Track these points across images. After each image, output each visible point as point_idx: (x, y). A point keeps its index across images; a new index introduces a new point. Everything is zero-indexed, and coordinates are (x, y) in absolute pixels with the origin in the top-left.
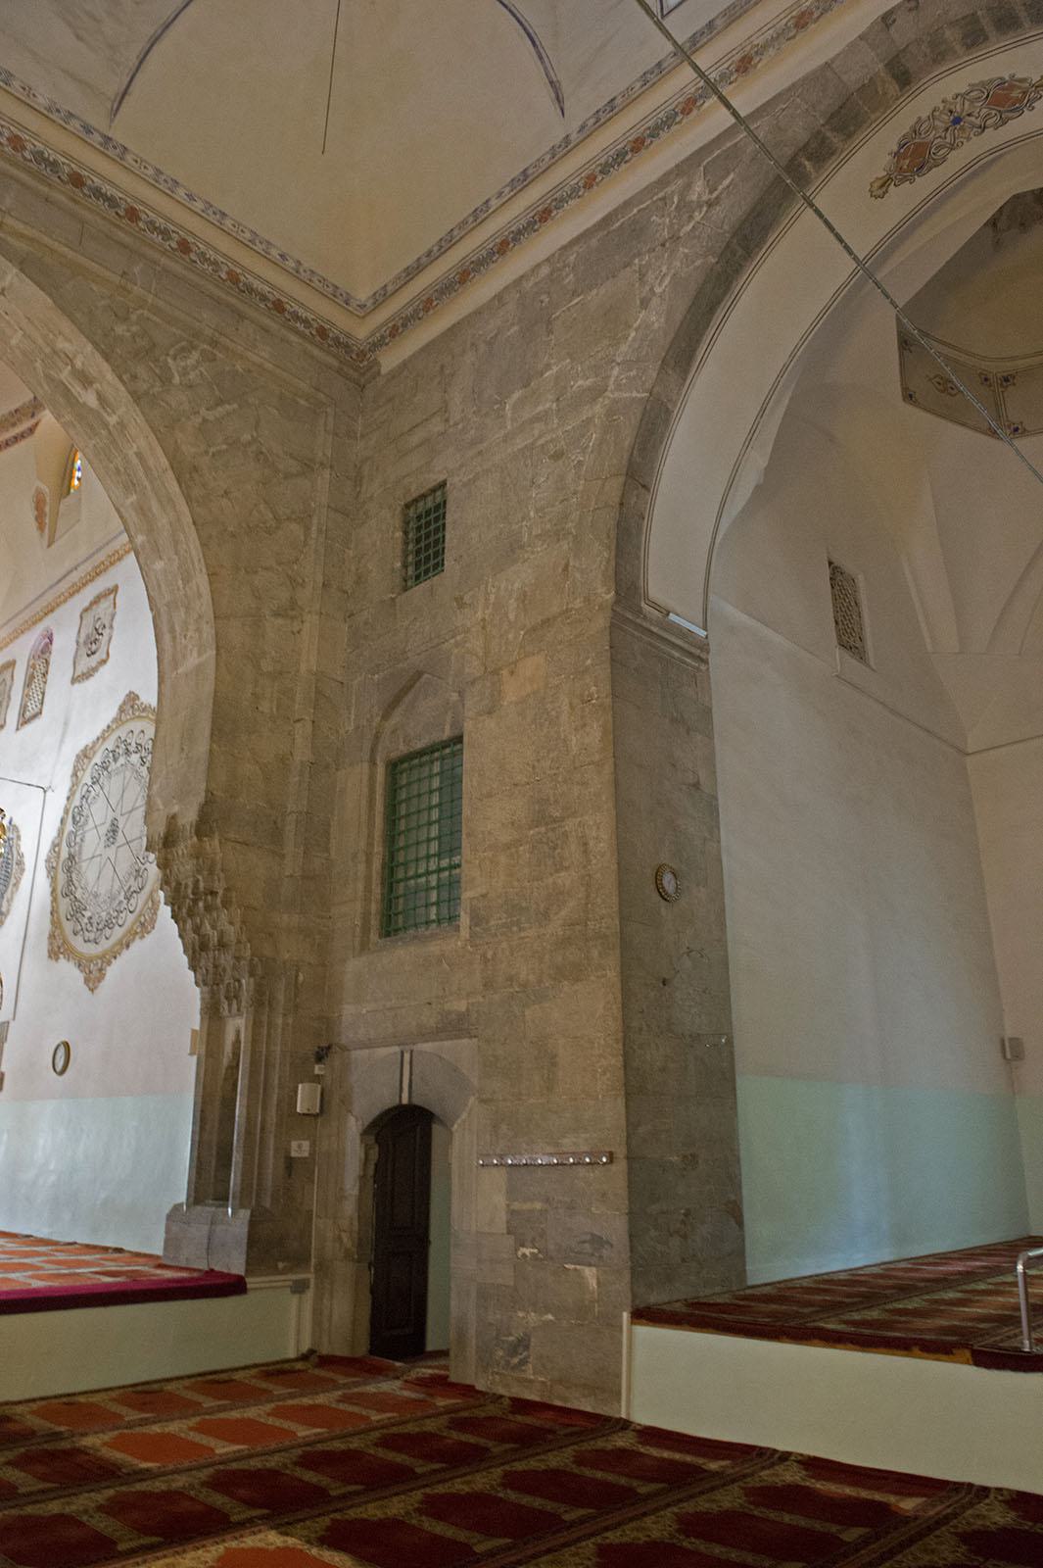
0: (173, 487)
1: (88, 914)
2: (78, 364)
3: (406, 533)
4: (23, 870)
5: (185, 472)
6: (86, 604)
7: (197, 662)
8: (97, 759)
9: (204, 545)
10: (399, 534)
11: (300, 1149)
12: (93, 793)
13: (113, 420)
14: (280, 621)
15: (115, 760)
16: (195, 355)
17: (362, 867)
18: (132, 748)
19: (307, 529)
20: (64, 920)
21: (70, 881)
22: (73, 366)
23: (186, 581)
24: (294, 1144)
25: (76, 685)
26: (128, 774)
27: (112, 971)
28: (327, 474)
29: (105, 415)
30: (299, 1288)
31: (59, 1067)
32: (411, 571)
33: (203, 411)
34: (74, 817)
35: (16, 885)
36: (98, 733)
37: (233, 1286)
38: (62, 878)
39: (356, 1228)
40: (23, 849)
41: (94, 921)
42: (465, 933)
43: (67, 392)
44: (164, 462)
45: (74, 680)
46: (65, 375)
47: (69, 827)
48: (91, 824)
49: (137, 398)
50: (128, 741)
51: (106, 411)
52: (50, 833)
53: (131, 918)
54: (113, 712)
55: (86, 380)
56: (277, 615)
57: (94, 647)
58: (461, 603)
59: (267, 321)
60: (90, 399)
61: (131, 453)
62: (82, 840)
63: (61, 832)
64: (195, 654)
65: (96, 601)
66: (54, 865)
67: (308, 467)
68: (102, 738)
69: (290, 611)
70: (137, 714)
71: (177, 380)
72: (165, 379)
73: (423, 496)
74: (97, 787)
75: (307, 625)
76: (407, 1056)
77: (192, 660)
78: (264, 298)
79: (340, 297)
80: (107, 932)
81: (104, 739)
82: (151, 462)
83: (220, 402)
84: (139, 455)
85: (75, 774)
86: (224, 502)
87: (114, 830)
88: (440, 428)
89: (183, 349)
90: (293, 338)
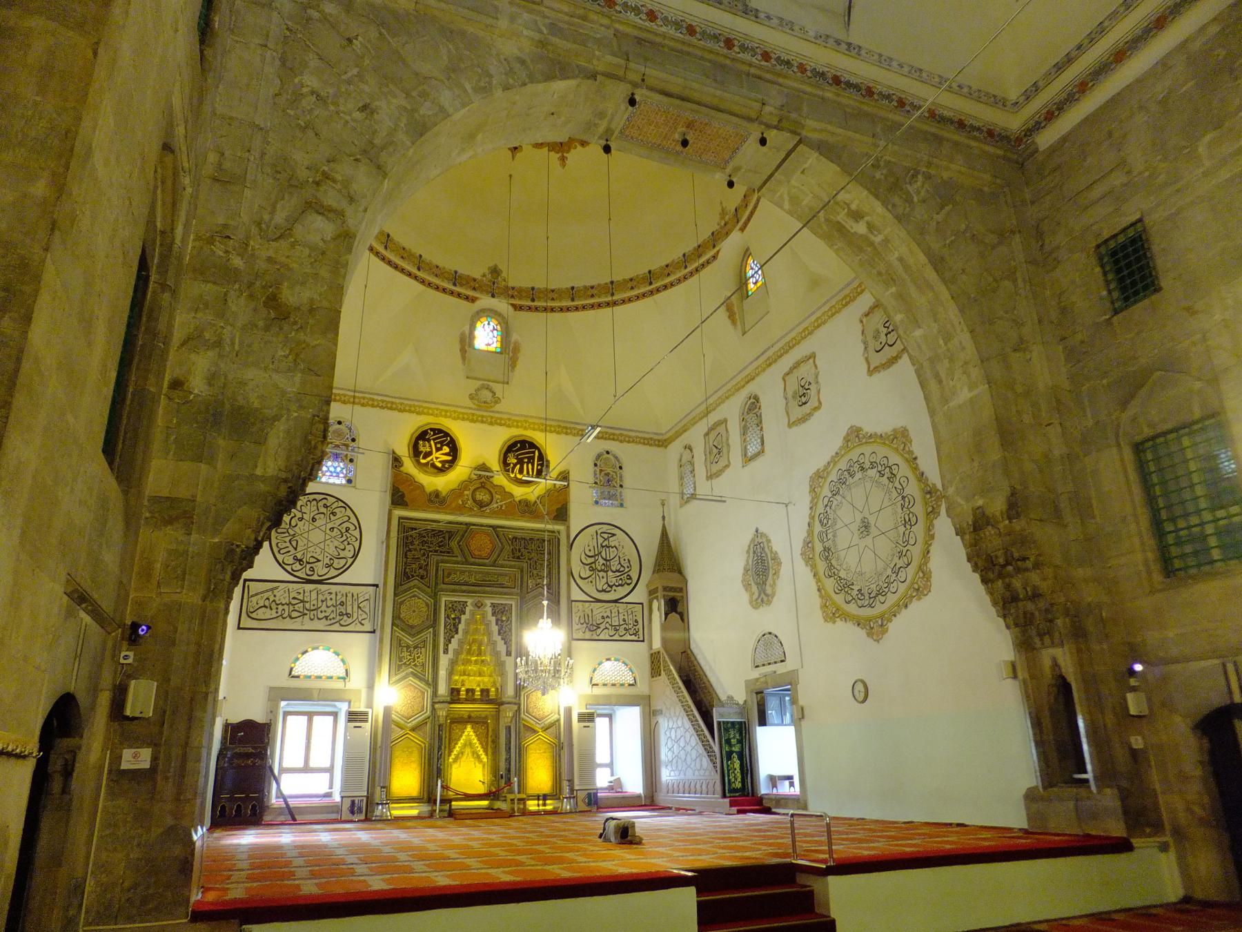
0: (931, 275)
1: (856, 588)
3: (1102, 266)
4: (780, 564)
5: (937, 262)
6: (786, 370)
7: (970, 395)
8: (833, 476)
9: (962, 311)
10: (1098, 270)
11: (1137, 742)
12: (835, 503)
13: (878, 239)
14: (1018, 355)
15: (852, 476)
16: (920, 177)
17: (1133, 527)
18: (867, 465)
19: (1015, 281)
20: (833, 594)
21: (831, 566)
22: (849, 209)
23: (948, 338)
24: (1132, 739)
25: (794, 428)
26: (868, 485)
27: (894, 626)
28: (1018, 236)
30: (1164, 848)
31: (861, 697)
32: (1116, 295)
33: (935, 216)
35: (776, 573)
36: (828, 458)
37: (1121, 846)
38: (821, 566)
39: (1206, 800)
40: (775, 549)
41: (865, 591)
43: (841, 229)
44: (922, 258)
45: (790, 425)
46: (841, 217)
47: (818, 528)
48: (839, 524)
49: (899, 218)
53: (903, 588)
54: (839, 442)
55: (857, 216)
56: (1015, 350)
57: (804, 399)
58: (1191, 311)
59: (956, 137)
60: (860, 228)
61: (893, 258)
63: (810, 532)
64: (966, 389)
65: (797, 365)
67: (1003, 236)
69: (1021, 346)
71: (915, 199)
72: (909, 200)
73: (1115, 236)
75: (1035, 354)
76: (1230, 667)
77: (964, 395)
78: (951, 121)
79: (999, 102)
80: (882, 599)
81: (835, 463)
82: (911, 261)
83: (942, 208)
84: (901, 259)
85: (813, 490)
86: (964, 277)
87: (865, 527)
88: (1124, 179)
89: (913, 176)
90: (973, 143)
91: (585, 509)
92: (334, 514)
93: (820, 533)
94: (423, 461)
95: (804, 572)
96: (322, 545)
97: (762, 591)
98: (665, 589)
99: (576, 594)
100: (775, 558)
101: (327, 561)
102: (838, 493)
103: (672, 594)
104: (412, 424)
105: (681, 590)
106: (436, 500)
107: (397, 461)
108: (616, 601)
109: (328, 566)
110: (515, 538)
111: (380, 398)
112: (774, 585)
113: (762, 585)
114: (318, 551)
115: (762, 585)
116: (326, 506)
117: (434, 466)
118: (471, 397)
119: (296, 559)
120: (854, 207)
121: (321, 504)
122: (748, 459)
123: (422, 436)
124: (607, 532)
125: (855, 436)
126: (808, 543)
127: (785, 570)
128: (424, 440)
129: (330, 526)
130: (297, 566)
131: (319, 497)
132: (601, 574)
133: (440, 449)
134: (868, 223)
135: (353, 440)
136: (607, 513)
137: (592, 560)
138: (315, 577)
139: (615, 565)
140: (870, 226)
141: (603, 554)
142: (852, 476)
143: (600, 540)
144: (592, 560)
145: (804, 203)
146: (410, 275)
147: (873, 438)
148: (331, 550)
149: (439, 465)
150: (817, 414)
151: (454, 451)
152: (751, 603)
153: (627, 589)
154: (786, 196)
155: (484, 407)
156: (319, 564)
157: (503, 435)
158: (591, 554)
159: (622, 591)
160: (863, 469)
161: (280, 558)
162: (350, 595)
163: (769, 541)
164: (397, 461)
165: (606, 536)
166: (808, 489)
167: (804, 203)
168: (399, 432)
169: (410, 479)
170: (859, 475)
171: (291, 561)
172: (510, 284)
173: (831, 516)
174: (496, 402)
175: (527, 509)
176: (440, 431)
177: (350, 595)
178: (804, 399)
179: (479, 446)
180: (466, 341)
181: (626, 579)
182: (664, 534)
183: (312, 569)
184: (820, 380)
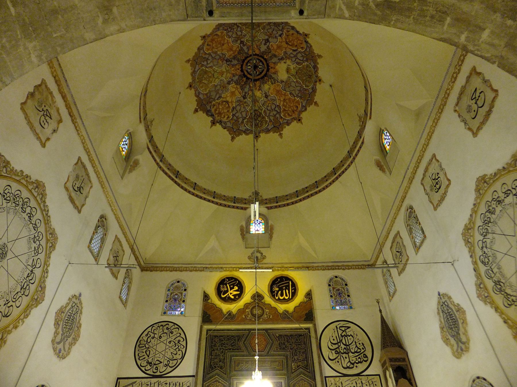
4: (464, 312)
8: (479, 222)
12: (488, 241)
34: (483, 262)
35: (464, 322)
38: (499, 299)
40: (456, 302)
47: (482, 269)
48: (499, 256)
50: (496, 197)
52: (470, 281)
62: (499, 269)
63: (478, 276)
66: (486, 295)
68: (474, 211)
70: (491, 181)
74: (490, 236)
85: (467, 242)
91: (326, 313)
92: (172, 333)
93: (486, 272)
94: (223, 296)
95: (487, 312)
96: (163, 353)
97: (459, 341)
98: (391, 360)
99: (328, 372)
100: (460, 309)
101: (166, 362)
102: (487, 232)
103: (398, 364)
104: (217, 276)
105: (404, 360)
106: (230, 317)
107: (206, 297)
108: (358, 375)
109: (166, 365)
110: (280, 336)
111: (199, 266)
112: (466, 333)
113: (456, 336)
114: (161, 356)
115: (456, 336)
116: (168, 329)
117: (229, 298)
118: (249, 258)
119: (148, 363)
121: (165, 328)
122: (417, 248)
123: (222, 282)
124: (343, 327)
125: (483, 182)
126: (480, 286)
127: (470, 316)
128: (223, 284)
129: (168, 340)
130: (148, 367)
131: (164, 324)
132: (344, 355)
133: (233, 288)
135: (185, 290)
136: (340, 313)
137: (337, 346)
138: (158, 374)
139: (353, 348)
141: (344, 341)
142: (493, 213)
143: (340, 332)
144: (337, 346)
146: (209, 201)
147: (497, 175)
148: (169, 355)
149: (233, 297)
150: (450, 190)
151: (241, 289)
152: (453, 354)
153: (366, 365)
155: (257, 261)
156: (162, 364)
157: (269, 275)
158: (335, 342)
159: (361, 367)
160: (500, 202)
161: (139, 362)
162: (178, 384)
163: (450, 298)
164: (206, 297)
165: (343, 329)
166: (462, 243)
168: (210, 282)
169: (214, 306)
170: (498, 209)
171: (145, 364)
172: (264, 198)
173: (490, 254)
174: (264, 258)
175: (286, 317)
176: (232, 278)
177: (178, 384)
178: (438, 186)
179: (256, 282)
180: (245, 231)
181: (363, 357)
182: (383, 322)
183: (157, 369)
184: (443, 167)
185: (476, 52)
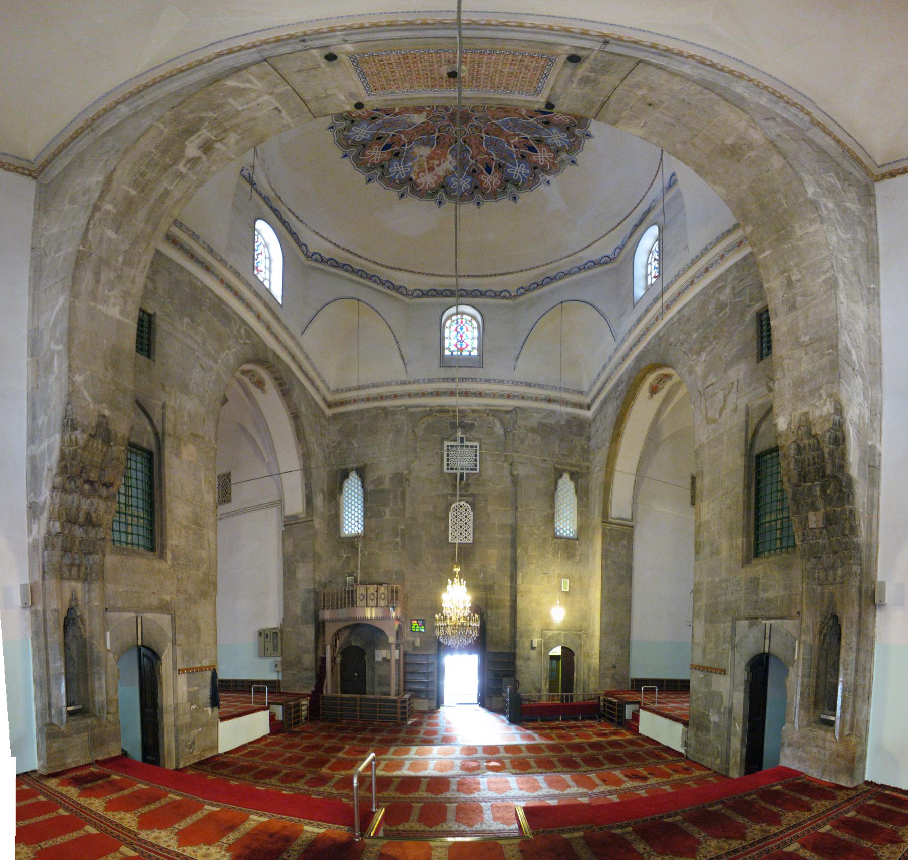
2: (218, 145)
13: (181, 167)
22: (217, 141)
29: (183, 162)
42: (169, 562)
46: (205, 132)
51: (186, 163)
60: (192, 150)
61: (165, 184)
84: (167, 192)
120: (218, 145)
134: (199, 158)
140: (194, 161)
145: (231, 101)
154: (248, 85)
167: (231, 101)
185: (92, 222)
